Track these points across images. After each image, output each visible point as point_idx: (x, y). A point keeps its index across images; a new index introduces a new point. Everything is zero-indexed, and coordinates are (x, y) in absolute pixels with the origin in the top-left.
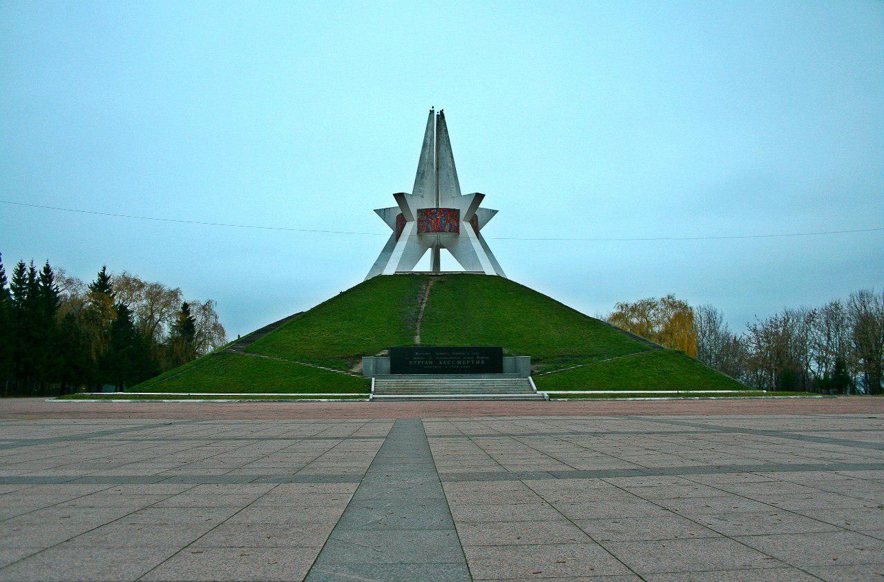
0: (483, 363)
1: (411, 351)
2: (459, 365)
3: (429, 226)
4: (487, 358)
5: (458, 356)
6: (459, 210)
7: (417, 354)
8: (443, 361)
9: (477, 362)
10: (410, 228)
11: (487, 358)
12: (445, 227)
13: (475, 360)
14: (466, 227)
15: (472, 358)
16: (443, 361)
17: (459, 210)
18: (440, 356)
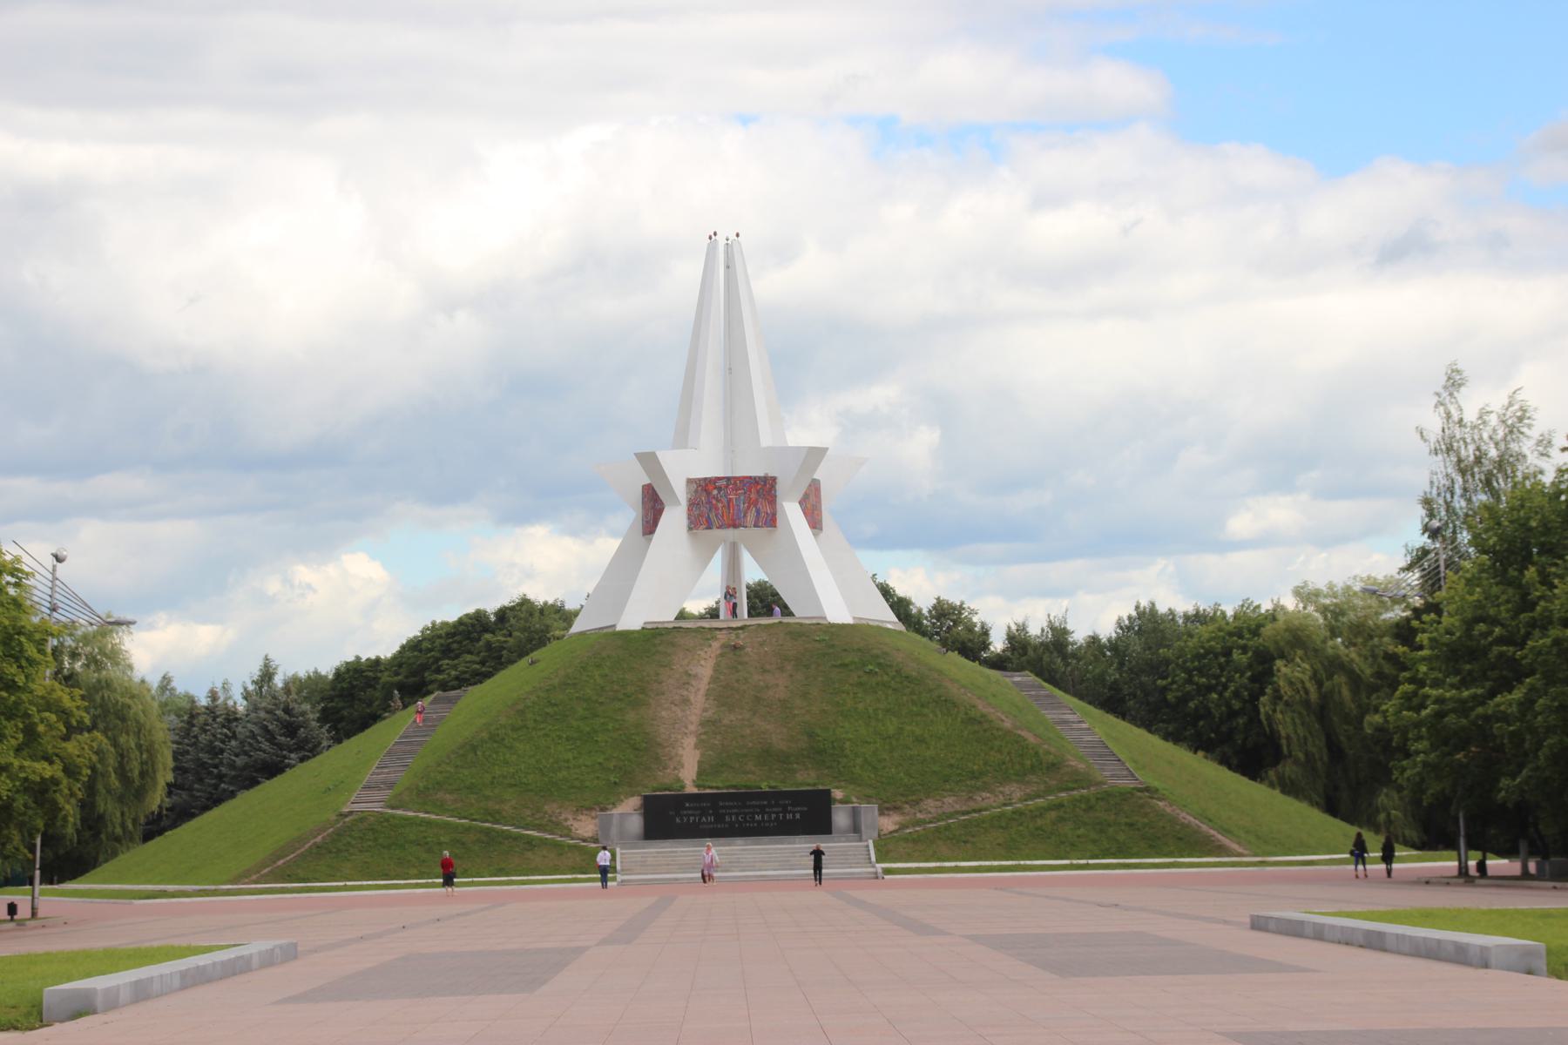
0: (798, 816)
1: (680, 801)
2: (759, 822)
3: (712, 515)
4: (805, 809)
5: (756, 806)
6: (774, 479)
7: (687, 805)
8: (730, 814)
9: (790, 816)
10: (674, 519)
11: (805, 809)
12: (745, 516)
13: (785, 811)
14: (791, 511)
15: (780, 809)
16: (730, 814)
17: (774, 479)
18: (723, 807)
